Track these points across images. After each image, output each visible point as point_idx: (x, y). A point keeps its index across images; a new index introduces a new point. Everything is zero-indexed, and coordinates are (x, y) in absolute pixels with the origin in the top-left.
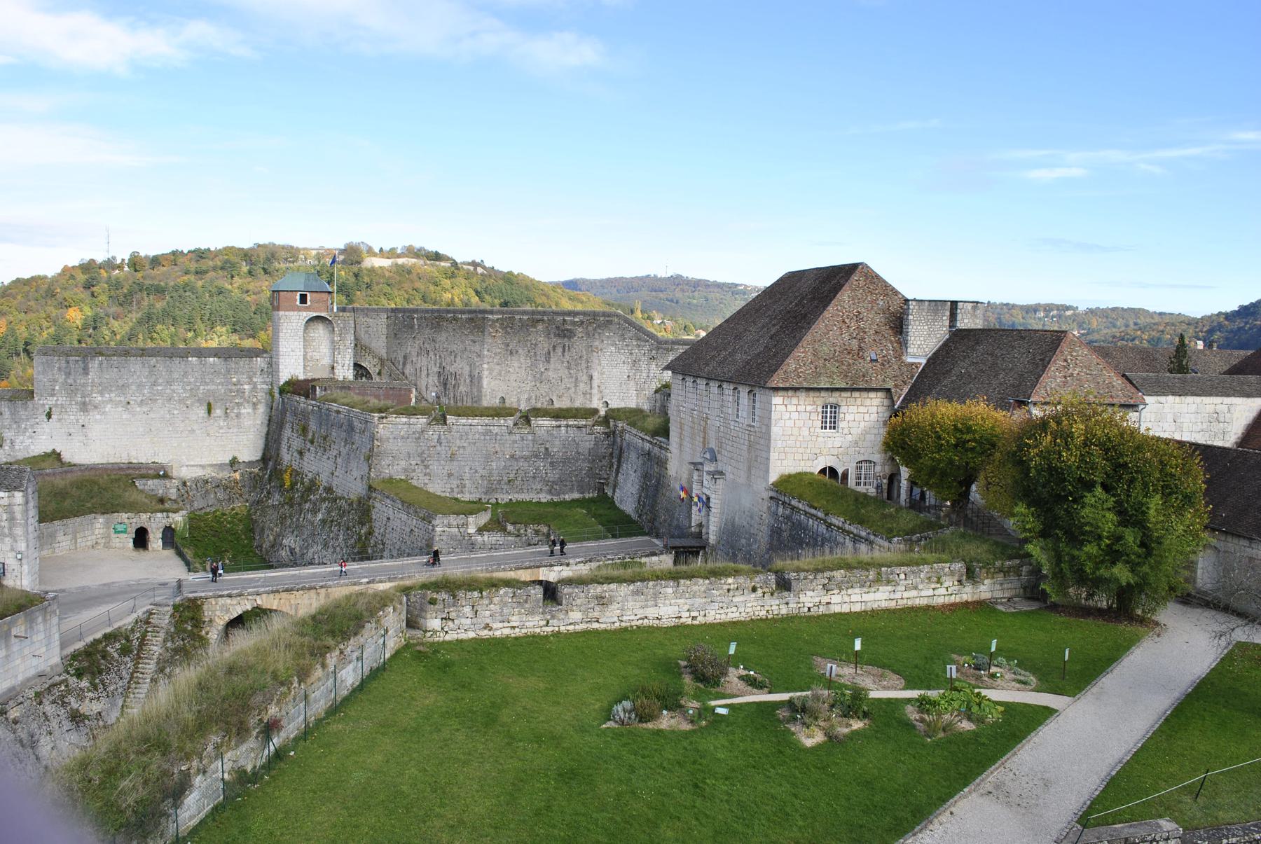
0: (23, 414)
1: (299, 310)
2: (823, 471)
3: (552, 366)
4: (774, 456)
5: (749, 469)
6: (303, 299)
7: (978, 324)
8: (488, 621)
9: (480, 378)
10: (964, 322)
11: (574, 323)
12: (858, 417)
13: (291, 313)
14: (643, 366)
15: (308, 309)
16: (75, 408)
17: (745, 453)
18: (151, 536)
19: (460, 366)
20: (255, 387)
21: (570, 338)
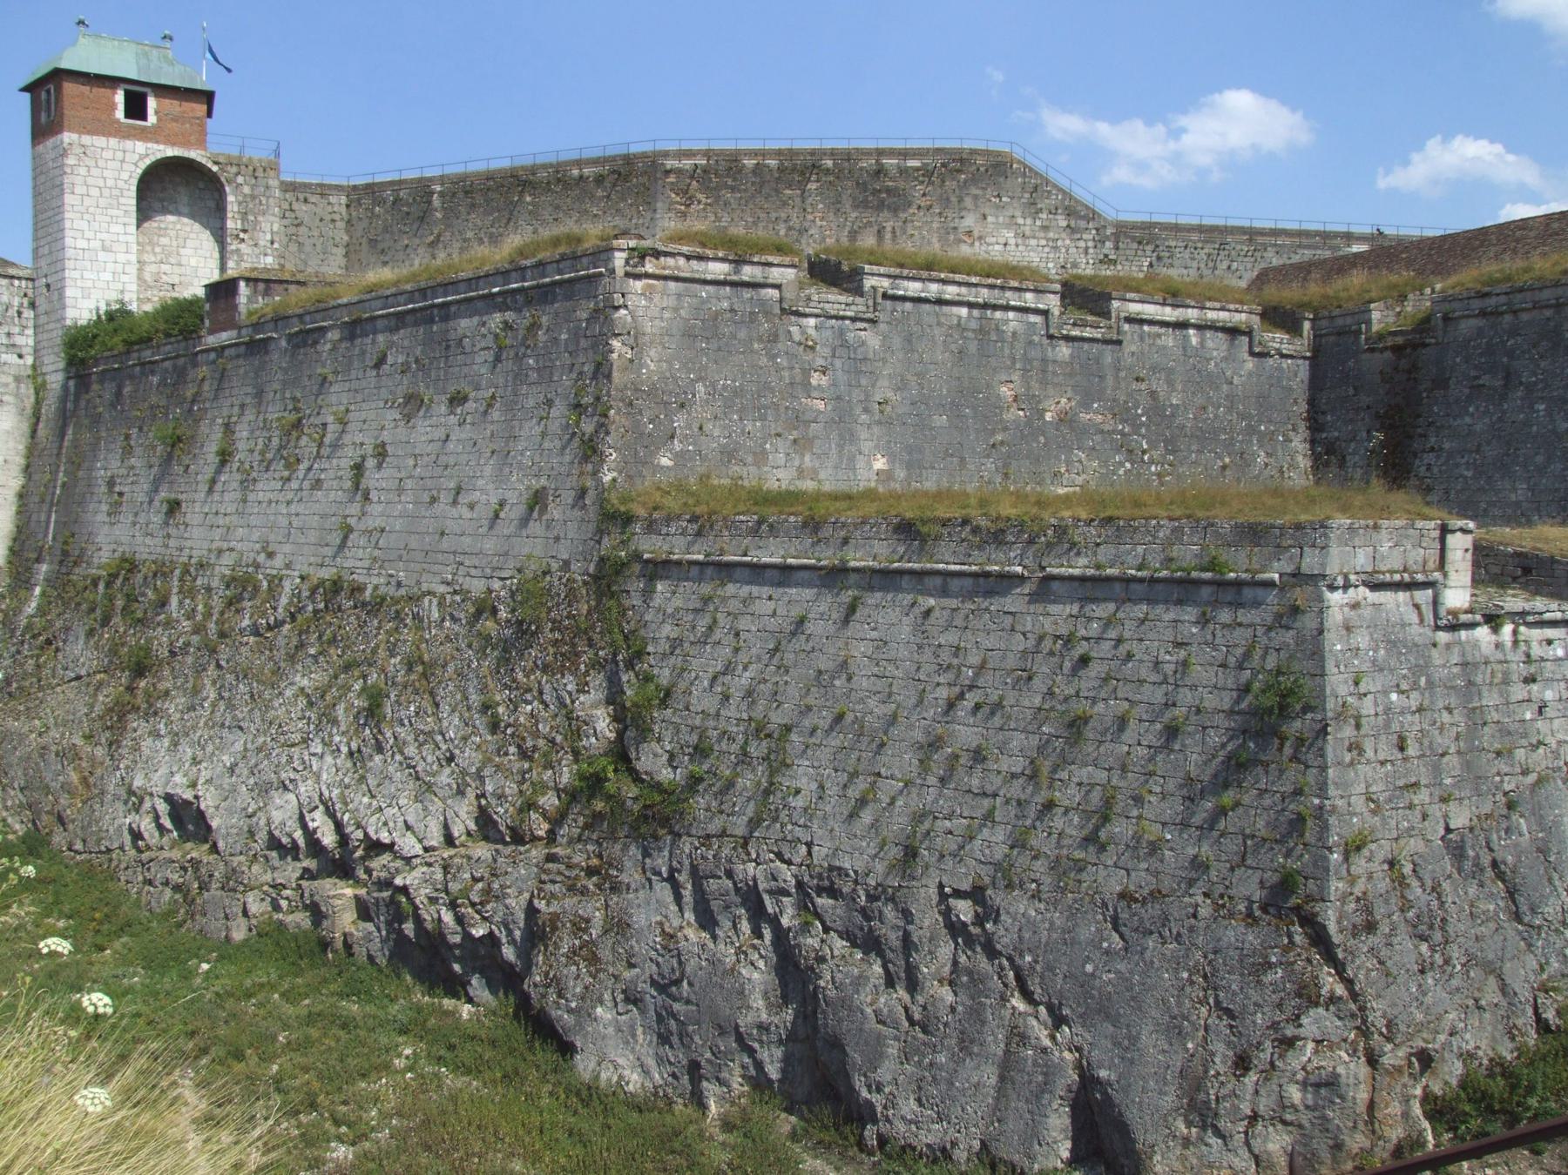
6: (136, 107)
11: (903, 171)
13: (100, 141)
21: (895, 210)
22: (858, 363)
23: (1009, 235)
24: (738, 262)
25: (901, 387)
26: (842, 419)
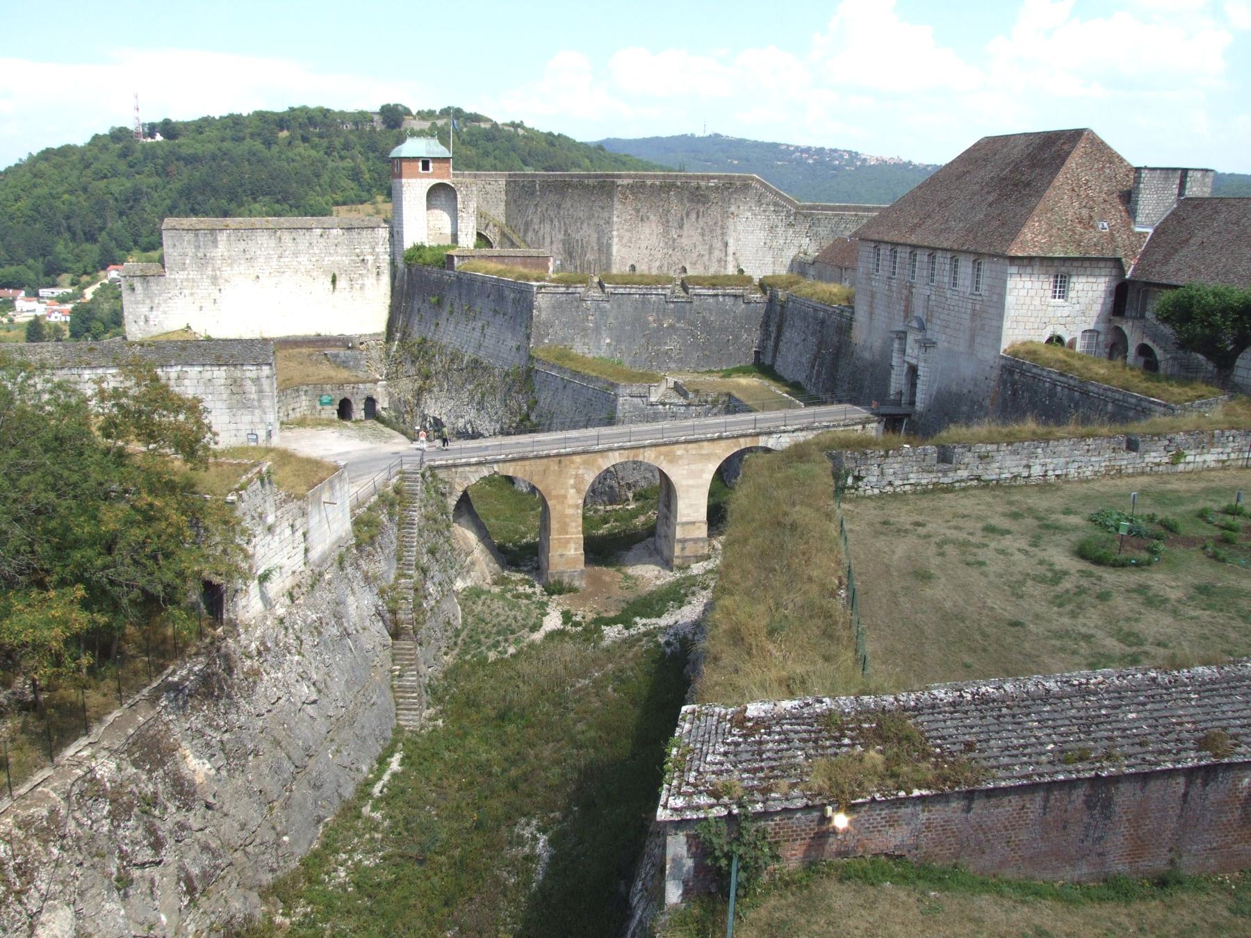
0: (154, 288)
1: (422, 176)
2: (1050, 341)
3: (685, 233)
4: (1007, 324)
5: (972, 338)
6: (426, 167)
7: (1206, 192)
8: (891, 478)
9: (609, 246)
10: (1193, 190)
11: (708, 188)
12: (1087, 287)
13: (414, 180)
14: (780, 230)
15: (428, 176)
16: (207, 282)
17: (967, 323)
18: (354, 407)
19: (587, 233)
20: (378, 255)
22: (603, 313)
23: (749, 214)
24: (568, 288)
25: (616, 318)
26: (597, 329)
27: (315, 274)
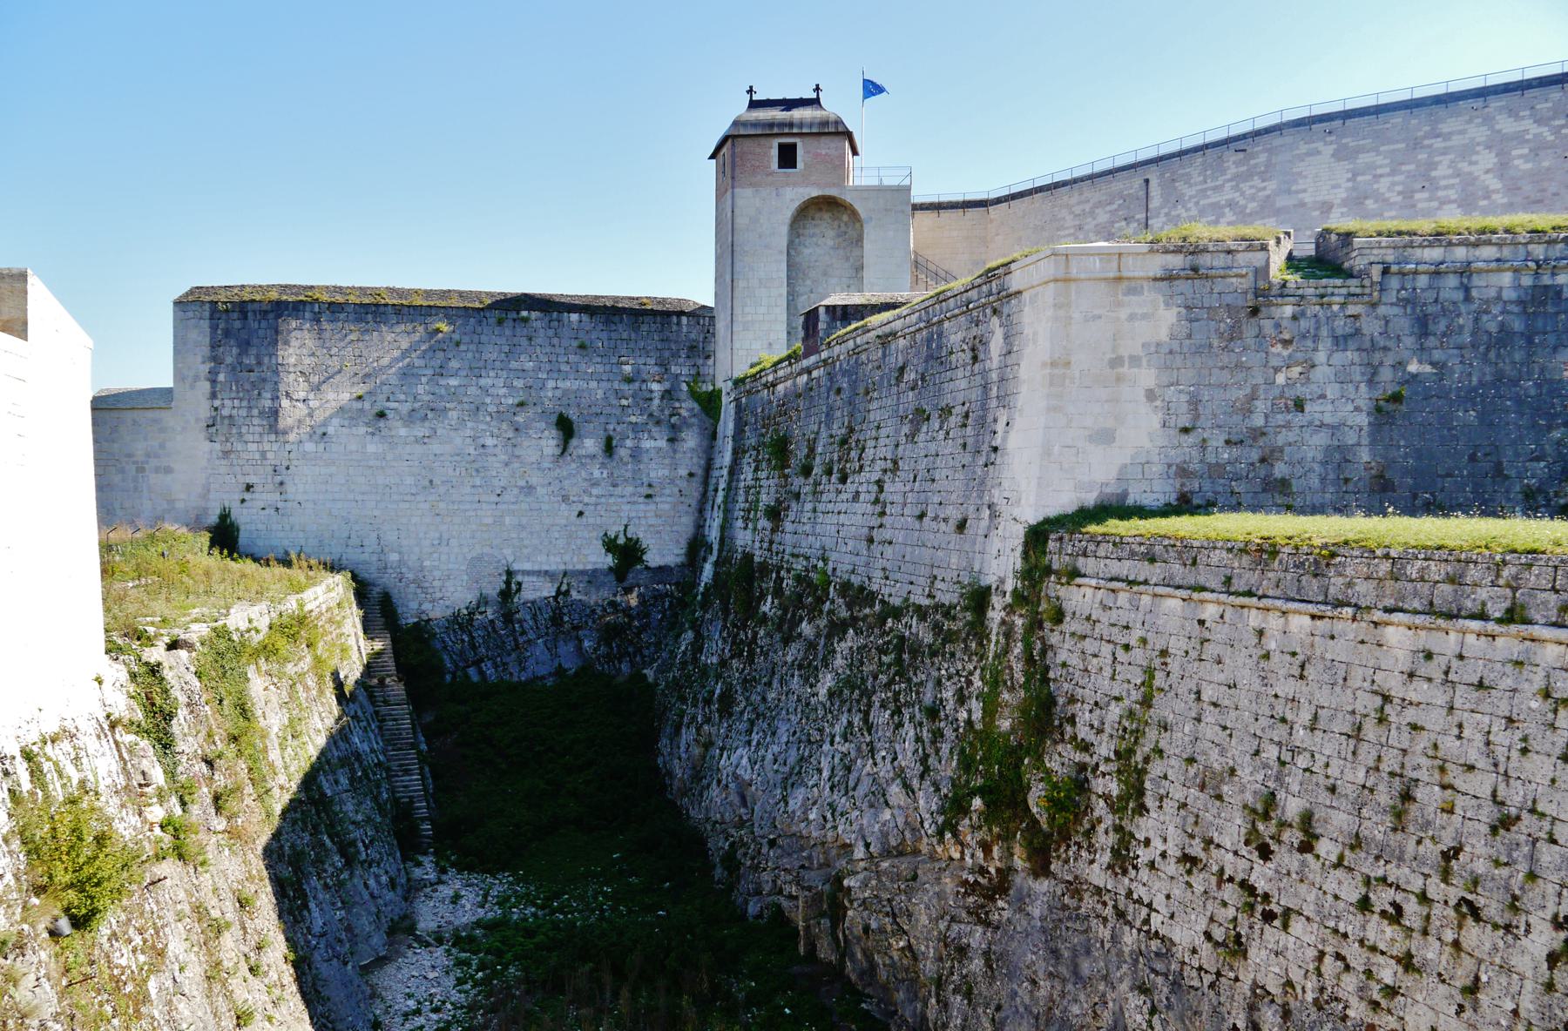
6: (788, 157)
27: (520, 419)
